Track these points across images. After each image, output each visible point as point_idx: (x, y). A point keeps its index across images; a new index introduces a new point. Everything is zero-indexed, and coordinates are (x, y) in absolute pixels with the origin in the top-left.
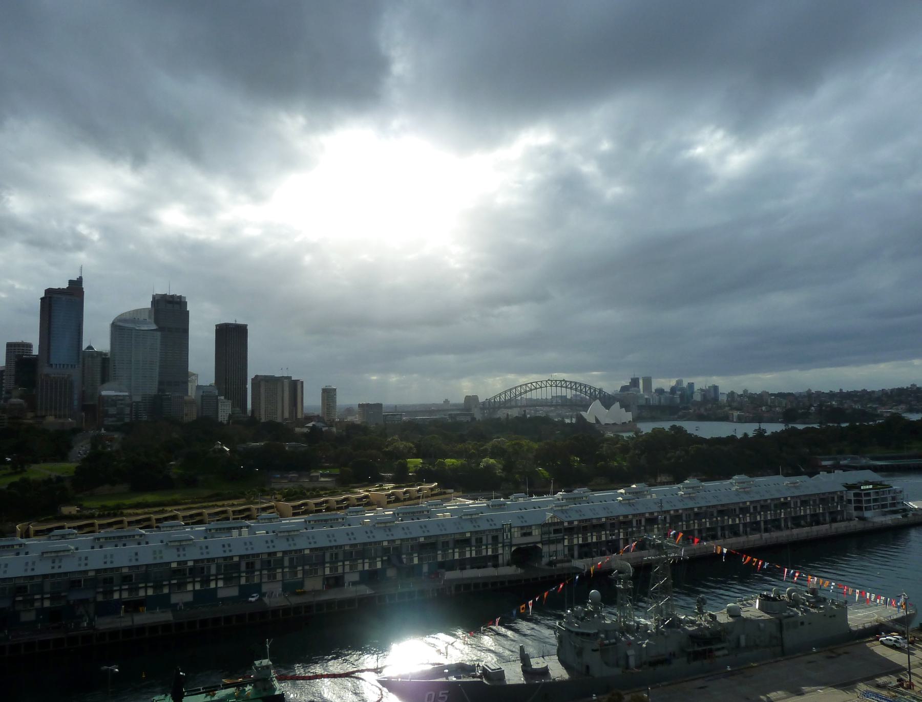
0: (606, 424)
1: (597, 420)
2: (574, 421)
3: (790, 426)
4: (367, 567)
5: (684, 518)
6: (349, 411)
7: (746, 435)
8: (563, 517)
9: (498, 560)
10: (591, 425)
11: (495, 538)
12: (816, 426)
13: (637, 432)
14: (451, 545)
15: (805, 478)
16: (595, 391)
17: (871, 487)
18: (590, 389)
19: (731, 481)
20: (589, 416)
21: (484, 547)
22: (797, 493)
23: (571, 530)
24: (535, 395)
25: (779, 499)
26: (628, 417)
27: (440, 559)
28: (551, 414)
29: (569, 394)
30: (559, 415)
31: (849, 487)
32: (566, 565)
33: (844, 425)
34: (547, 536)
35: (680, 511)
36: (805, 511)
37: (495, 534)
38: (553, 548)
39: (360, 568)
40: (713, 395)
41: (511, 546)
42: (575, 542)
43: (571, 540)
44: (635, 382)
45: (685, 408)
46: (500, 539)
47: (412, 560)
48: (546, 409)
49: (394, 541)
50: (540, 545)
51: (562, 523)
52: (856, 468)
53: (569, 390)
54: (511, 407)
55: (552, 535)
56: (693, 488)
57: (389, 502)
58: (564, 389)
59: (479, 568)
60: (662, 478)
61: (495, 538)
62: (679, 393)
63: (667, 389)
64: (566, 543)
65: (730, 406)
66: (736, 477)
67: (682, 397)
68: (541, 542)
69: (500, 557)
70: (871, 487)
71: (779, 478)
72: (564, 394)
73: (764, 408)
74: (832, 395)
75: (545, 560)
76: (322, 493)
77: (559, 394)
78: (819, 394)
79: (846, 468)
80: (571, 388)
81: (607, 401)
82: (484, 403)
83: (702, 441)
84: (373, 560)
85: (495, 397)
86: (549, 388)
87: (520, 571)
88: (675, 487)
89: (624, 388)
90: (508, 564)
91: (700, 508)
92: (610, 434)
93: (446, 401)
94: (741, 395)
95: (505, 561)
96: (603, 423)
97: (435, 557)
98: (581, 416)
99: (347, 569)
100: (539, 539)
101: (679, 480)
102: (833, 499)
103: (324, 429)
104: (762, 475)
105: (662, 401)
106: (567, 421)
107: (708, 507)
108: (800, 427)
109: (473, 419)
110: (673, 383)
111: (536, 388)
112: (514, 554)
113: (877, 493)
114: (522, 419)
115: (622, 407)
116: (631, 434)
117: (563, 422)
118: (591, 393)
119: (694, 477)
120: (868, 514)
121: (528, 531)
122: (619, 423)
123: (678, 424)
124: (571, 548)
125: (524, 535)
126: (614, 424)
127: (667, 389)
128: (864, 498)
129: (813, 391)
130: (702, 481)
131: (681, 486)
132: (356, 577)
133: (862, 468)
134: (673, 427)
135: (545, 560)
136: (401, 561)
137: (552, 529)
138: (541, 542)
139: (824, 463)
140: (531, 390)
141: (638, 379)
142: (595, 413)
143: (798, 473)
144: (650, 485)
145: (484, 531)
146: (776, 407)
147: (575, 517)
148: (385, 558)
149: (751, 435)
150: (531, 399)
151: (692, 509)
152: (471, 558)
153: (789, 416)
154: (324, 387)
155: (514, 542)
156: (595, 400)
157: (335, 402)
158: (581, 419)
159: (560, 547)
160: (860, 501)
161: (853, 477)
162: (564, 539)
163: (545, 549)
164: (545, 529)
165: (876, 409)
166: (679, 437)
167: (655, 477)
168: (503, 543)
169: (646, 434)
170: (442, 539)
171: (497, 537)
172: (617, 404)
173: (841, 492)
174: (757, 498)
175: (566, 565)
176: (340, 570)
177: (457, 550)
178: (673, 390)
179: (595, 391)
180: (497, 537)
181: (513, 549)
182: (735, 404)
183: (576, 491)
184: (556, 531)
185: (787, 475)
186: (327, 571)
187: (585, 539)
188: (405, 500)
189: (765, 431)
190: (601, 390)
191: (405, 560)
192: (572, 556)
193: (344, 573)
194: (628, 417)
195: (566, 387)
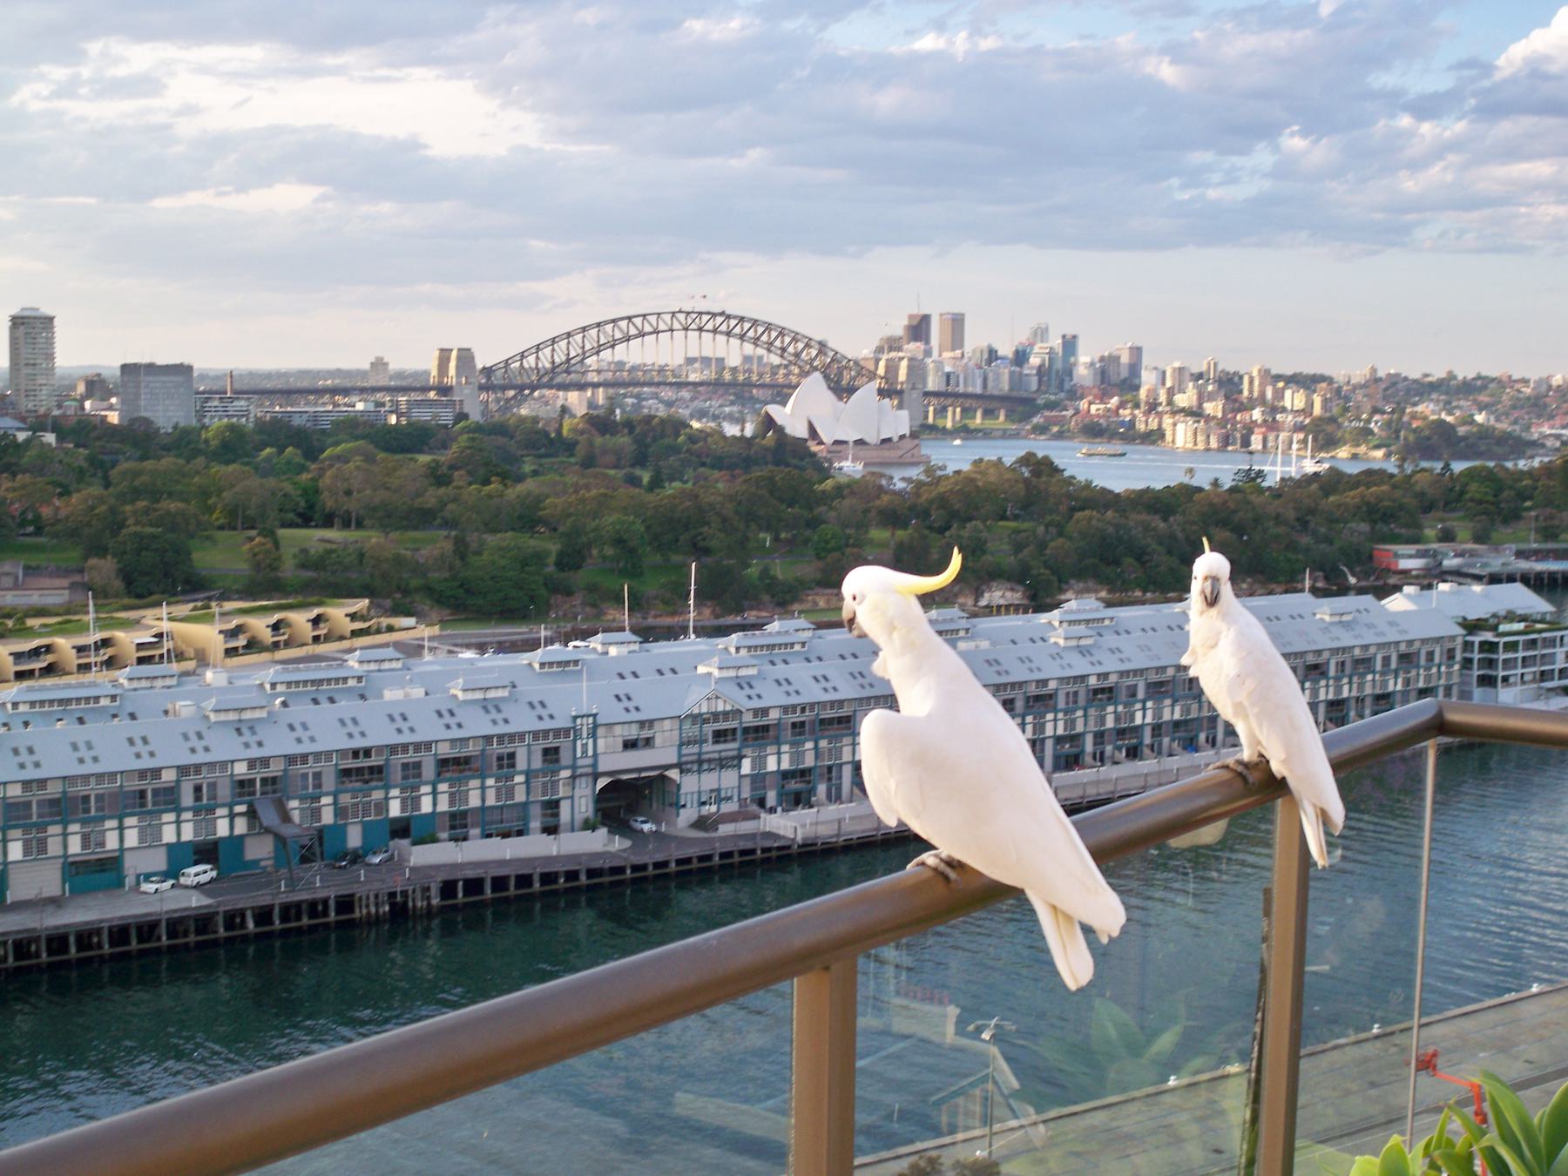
0: (837, 442)
4: (188, 834)
5: (1061, 704)
6: (96, 385)
7: (1216, 483)
8: (740, 700)
9: (557, 815)
11: (551, 754)
12: (1391, 467)
14: (429, 770)
15: (1368, 600)
17: (1521, 626)
20: (791, 417)
21: (519, 779)
22: (1347, 640)
23: (760, 734)
24: (635, 354)
26: (898, 422)
27: (395, 810)
28: (684, 412)
29: (733, 353)
31: (1472, 626)
32: (746, 827)
33: (1458, 467)
34: (695, 749)
35: (1052, 685)
36: (1361, 686)
37: (551, 742)
38: (709, 780)
39: (169, 835)
40: (1124, 373)
41: (596, 776)
42: (772, 764)
43: (759, 762)
44: (919, 329)
45: (1051, 406)
46: (565, 757)
47: (316, 813)
48: (667, 393)
49: (265, 762)
50: (673, 774)
51: (737, 713)
52: (1478, 578)
53: (735, 342)
54: (564, 387)
55: (710, 748)
57: (231, 652)
58: (721, 339)
59: (505, 835)
61: (551, 754)
62: (1034, 361)
63: (1006, 350)
64: (746, 767)
68: (681, 766)
69: (565, 808)
70: (1521, 626)
74: (1424, 389)
75: (687, 816)
76: (30, 622)
78: (1394, 381)
79: (1458, 575)
80: (742, 337)
82: (488, 371)
84: (204, 811)
85: (523, 355)
86: (679, 335)
87: (619, 844)
88: (1043, 618)
90: (589, 826)
91: (1103, 676)
92: (850, 467)
93: (379, 364)
95: (579, 818)
97: (383, 806)
99: (132, 838)
100: (675, 761)
101: (1040, 601)
102: (1430, 655)
103: (22, 436)
106: (731, 430)
107: (1123, 674)
109: (462, 416)
111: (642, 335)
112: (602, 797)
113: (1534, 642)
114: (600, 423)
116: (915, 473)
120: (1506, 695)
121: (646, 734)
122: (872, 438)
123: (1042, 447)
124: (758, 779)
125: (630, 745)
126: (860, 442)
127: (1006, 350)
128: (1502, 656)
129: (1381, 374)
130: (1109, 604)
131: (1056, 614)
132: (159, 861)
133: (1494, 579)
134: (1028, 460)
135: (687, 816)
136: (286, 818)
137: (709, 729)
138: (681, 766)
139: (1404, 564)
140: (628, 339)
141: (925, 319)
142: (805, 411)
145: (521, 736)
147: (773, 698)
148: (241, 808)
149: (1227, 483)
150: (620, 365)
151: (1083, 678)
152: (483, 809)
153: (1323, 434)
154: (14, 311)
155: (601, 769)
156: (808, 374)
157: (50, 357)
158: (769, 422)
159: (728, 779)
160: (1491, 663)
161: (1480, 600)
162: (740, 757)
163: (690, 785)
164: (691, 730)
165: (1528, 428)
166: (1039, 487)
168: (574, 767)
170: (401, 758)
171: (556, 750)
173: (1453, 638)
175: (746, 827)
176: (112, 842)
177: (443, 787)
178: (1021, 357)
180: (556, 750)
181: (602, 783)
182: (1182, 400)
184: (719, 736)
185: (1317, 592)
186: (75, 846)
187: (797, 756)
188: (276, 646)
189: (1260, 474)
190: (822, 346)
191: (296, 816)
192: (761, 803)
193: (122, 850)
194: (898, 422)
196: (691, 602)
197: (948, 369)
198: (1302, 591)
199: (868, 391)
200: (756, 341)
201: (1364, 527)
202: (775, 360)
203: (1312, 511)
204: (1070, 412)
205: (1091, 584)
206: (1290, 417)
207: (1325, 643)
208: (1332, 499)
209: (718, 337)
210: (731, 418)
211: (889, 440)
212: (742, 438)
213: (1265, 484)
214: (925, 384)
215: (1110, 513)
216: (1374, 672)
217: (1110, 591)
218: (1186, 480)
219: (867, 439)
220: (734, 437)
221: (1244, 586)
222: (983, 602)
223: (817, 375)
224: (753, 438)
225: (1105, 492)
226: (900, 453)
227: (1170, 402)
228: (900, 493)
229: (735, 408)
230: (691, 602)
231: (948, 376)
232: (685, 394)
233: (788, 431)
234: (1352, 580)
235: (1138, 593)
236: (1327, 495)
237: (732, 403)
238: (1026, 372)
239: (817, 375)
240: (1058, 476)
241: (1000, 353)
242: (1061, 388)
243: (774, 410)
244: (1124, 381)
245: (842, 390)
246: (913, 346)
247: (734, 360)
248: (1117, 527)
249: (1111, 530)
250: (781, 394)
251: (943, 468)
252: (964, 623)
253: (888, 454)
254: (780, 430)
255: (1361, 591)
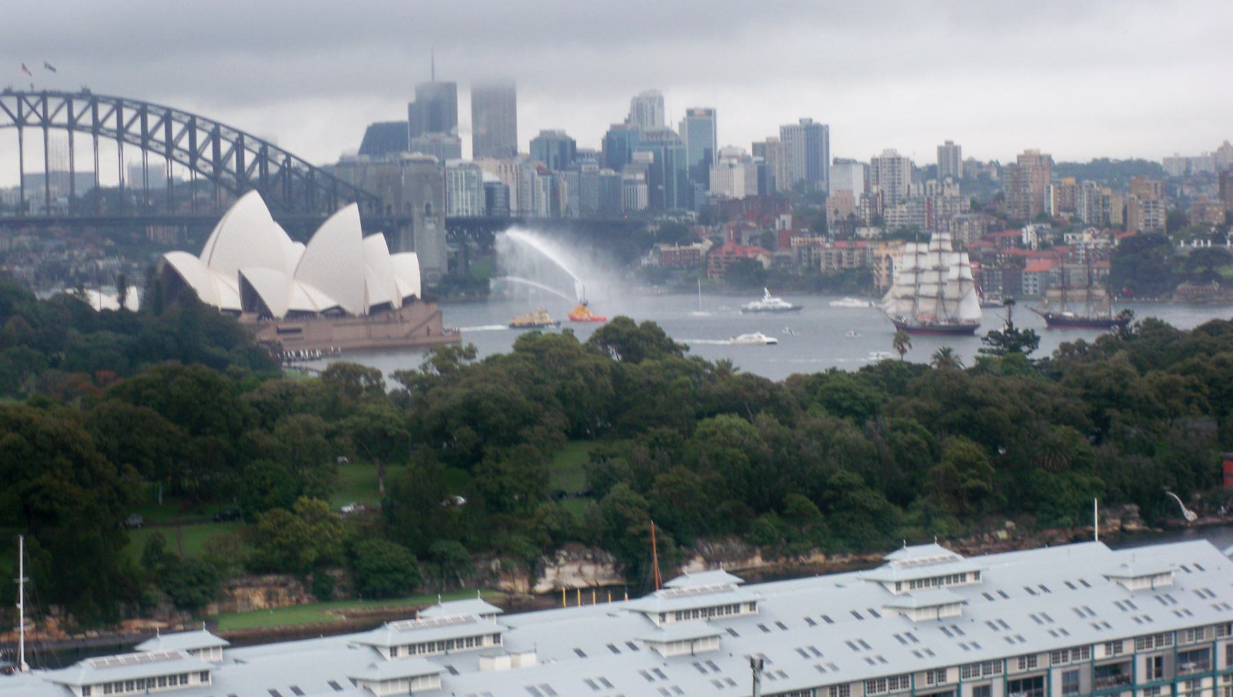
0: (294, 314)
1: (249, 294)
2: (134, 300)
3: (1141, 316)
10: (219, 325)
13: (447, 355)
16: (239, 147)
18: (215, 137)
19: (878, 573)
22: (1164, 620)
25: (1086, 649)
26: (400, 274)
29: (109, 165)
30: (56, 273)
40: (800, 172)
53: (108, 146)
56: (708, 611)
60: (567, 572)
65: (877, 221)
66: (908, 554)
67: (654, 174)
71: (1091, 556)
72: (83, 164)
73: (1028, 234)
77: (60, 164)
80: (121, 135)
81: (302, 202)
83: (750, 396)
89: (380, 138)
94: (931, 171)
96: (278, 309)
98: (174, 278)
101: (635, 581)
104: (1014, 545)
105: (565, 199)
106: (102, 300)
108: (1184, 319)
110: (617, 112)
115: (368, 228)
117: (83, 307)
118: (219, 162)
119: (711, 562)
122: (355, 307)
126: (337, 313)
130: (750, 578)
131: (655, 602)
141: (450, 90)
143: (1171, 531)
144: (511, 606)
146: (1075, 225)
156: (239, 193)
158: (170, 288)
167: (534, 573)
169: (492, 360)
172: (349, 216)
174: (994, 647)
178: (617, 146)
179: (239, 147)
182: (897, 215)
183: (152, 647)
185: (1118, 540)
194: (400, 274)
195: (96, 129)
196: (21, 606)
197: (488, 177)
198: (1090, 538)
199: (349, 216)
200: (145, 141)
201: (1206, 424)
202: (182, 173)
203: (1114, 398)
204: (706, 245)
205: (735, 545)
206: (1086, 237)
207: (1124, 627)
208: (1150, 374)
209: (77, 135)
210: (99, 281)
211: (385, 307)
212: (123, 310)
213: (1037, 355)
214: (449, 207)
215: (762, 417)
216: (1214, 675)
217: (765, 558)
218: (893, 355)
219: (348, 307)
220: (106, 312)
221: (1002, 535)
222: (543, 586)
223: (253, 202)
224: (141, 312)
225: (753, 383)
226: (406, 328)
227: (877, 221)
228: (399, 400)
229: (115, 262)
230: (21, 606)
231: (490, 190)
232: (24, 239)
233: (205, 296)
234: (1190, 516)
235: (818, 558)
236: (1142, 371)
237: (110, 253)
238: (626, 176)
239: (253, 202)
240: (671, 358)
241: (580, 146)
242: (687, 199)
243: (180, 261)
244: (798, 187)
245: (300, 221)
246: (426, 138)
247: (109, 179)
248: (776, 441)
249: (765, 447)
250: (196, 235)
251: (471, 352)
252: (492, 625)
253: (381, 331)
254: (189, 295)
255: (1201, 531)
